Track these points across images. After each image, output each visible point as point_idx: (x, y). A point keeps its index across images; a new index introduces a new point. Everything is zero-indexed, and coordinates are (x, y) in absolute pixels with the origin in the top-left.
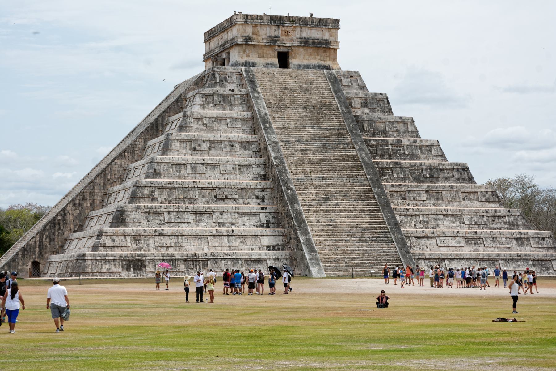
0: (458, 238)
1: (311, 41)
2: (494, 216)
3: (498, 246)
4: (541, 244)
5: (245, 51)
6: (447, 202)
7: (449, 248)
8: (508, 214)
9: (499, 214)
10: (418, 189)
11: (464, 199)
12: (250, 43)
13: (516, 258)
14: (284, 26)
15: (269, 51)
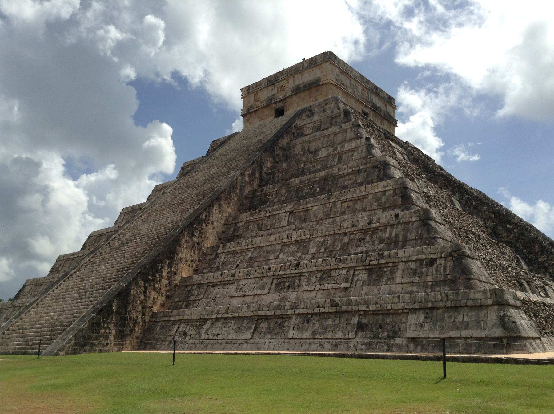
0: (265, 279)
1: (301, 86)
2: (365, 231)
3: (326, 286)
4: (421, 275)
5: (249, 120)
6: (315, 223)
7: (242, 299)
8: (392, 222)
9: (373, 226)
10: (280, 212)
11: (343, 213)
12: (251, 111)
13: (326, 310)
14: (278, 82)
15: (267, 112)
